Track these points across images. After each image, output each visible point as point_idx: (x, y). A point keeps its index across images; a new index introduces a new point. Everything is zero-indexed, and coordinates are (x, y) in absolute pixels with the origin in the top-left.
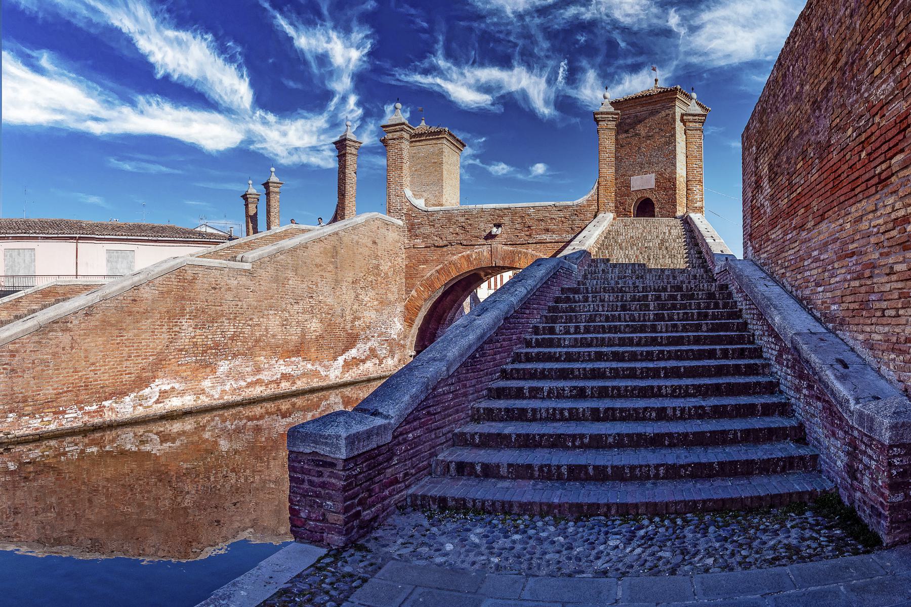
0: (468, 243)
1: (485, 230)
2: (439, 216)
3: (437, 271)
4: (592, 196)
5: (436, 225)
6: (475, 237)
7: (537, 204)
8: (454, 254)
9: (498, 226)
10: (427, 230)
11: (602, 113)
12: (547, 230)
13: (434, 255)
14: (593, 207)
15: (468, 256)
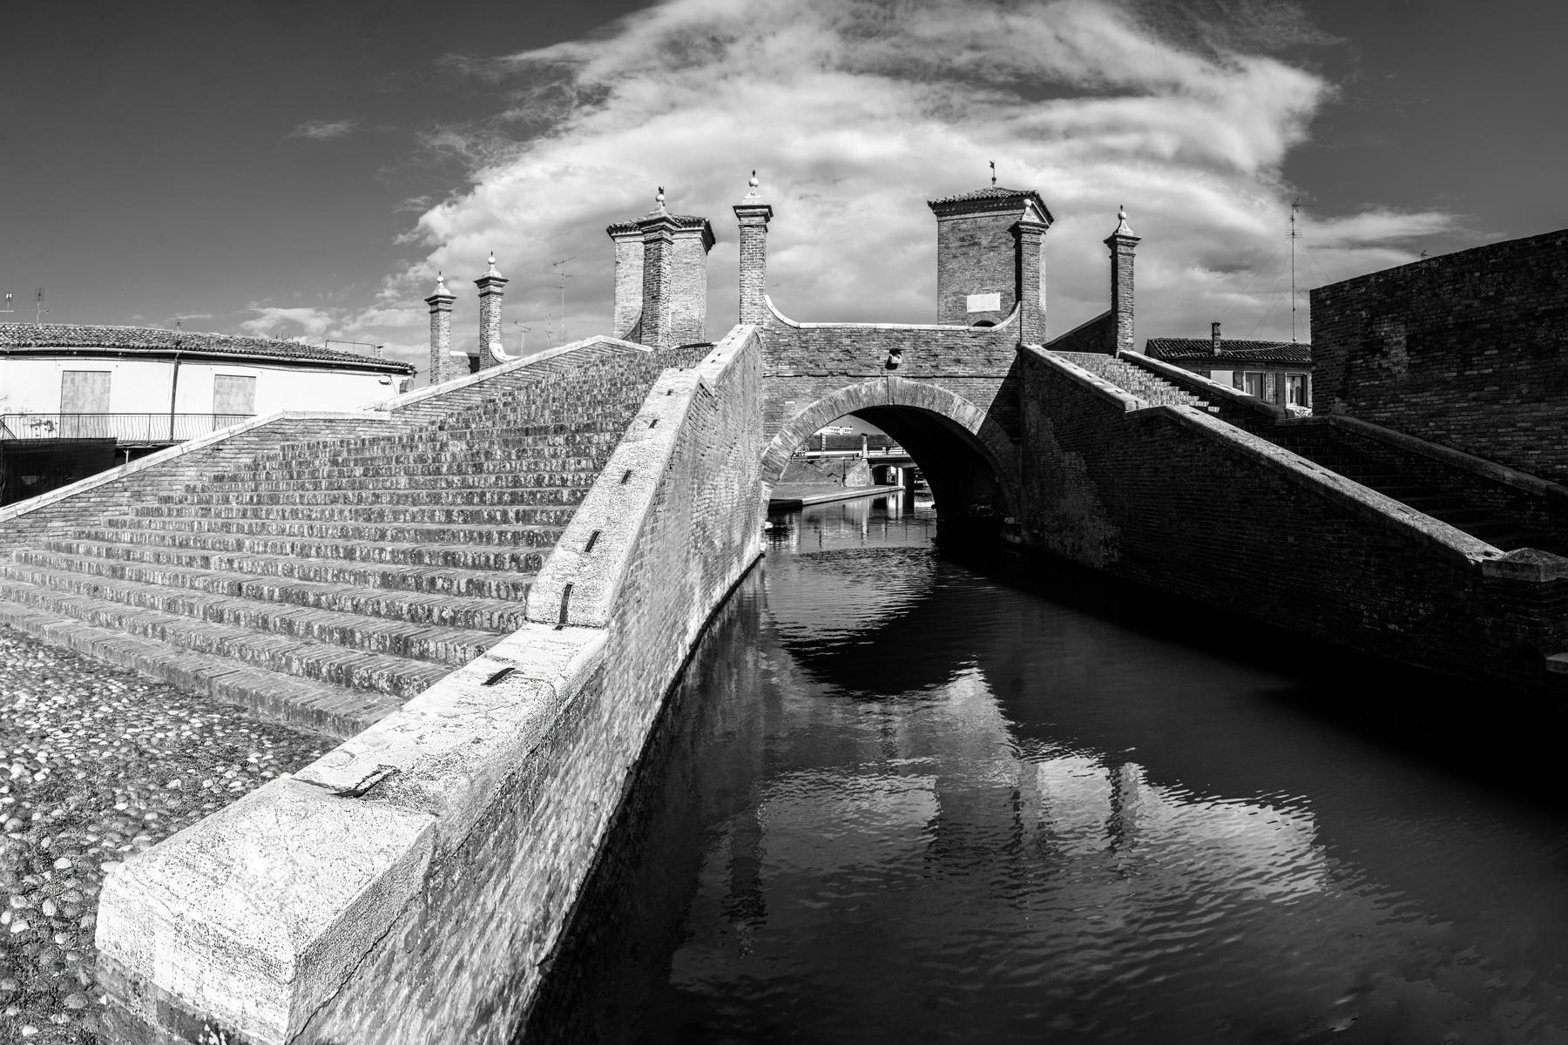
0: (856, 374)
1: (878, 358)
2: (815, 336)
3: (811, 409)
4: (1013, 322)
5: (811, 348)
6: (866, 365)
7: (947, 327)
8: (835, 388)
9: (895, 352)
10: (798, 353)
11: (1027, 224)
12: (958, 361)
13: (808, 386)
14: (1014, 336)
15: (855, 390)
